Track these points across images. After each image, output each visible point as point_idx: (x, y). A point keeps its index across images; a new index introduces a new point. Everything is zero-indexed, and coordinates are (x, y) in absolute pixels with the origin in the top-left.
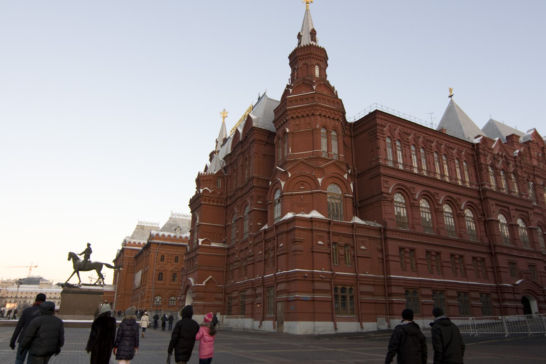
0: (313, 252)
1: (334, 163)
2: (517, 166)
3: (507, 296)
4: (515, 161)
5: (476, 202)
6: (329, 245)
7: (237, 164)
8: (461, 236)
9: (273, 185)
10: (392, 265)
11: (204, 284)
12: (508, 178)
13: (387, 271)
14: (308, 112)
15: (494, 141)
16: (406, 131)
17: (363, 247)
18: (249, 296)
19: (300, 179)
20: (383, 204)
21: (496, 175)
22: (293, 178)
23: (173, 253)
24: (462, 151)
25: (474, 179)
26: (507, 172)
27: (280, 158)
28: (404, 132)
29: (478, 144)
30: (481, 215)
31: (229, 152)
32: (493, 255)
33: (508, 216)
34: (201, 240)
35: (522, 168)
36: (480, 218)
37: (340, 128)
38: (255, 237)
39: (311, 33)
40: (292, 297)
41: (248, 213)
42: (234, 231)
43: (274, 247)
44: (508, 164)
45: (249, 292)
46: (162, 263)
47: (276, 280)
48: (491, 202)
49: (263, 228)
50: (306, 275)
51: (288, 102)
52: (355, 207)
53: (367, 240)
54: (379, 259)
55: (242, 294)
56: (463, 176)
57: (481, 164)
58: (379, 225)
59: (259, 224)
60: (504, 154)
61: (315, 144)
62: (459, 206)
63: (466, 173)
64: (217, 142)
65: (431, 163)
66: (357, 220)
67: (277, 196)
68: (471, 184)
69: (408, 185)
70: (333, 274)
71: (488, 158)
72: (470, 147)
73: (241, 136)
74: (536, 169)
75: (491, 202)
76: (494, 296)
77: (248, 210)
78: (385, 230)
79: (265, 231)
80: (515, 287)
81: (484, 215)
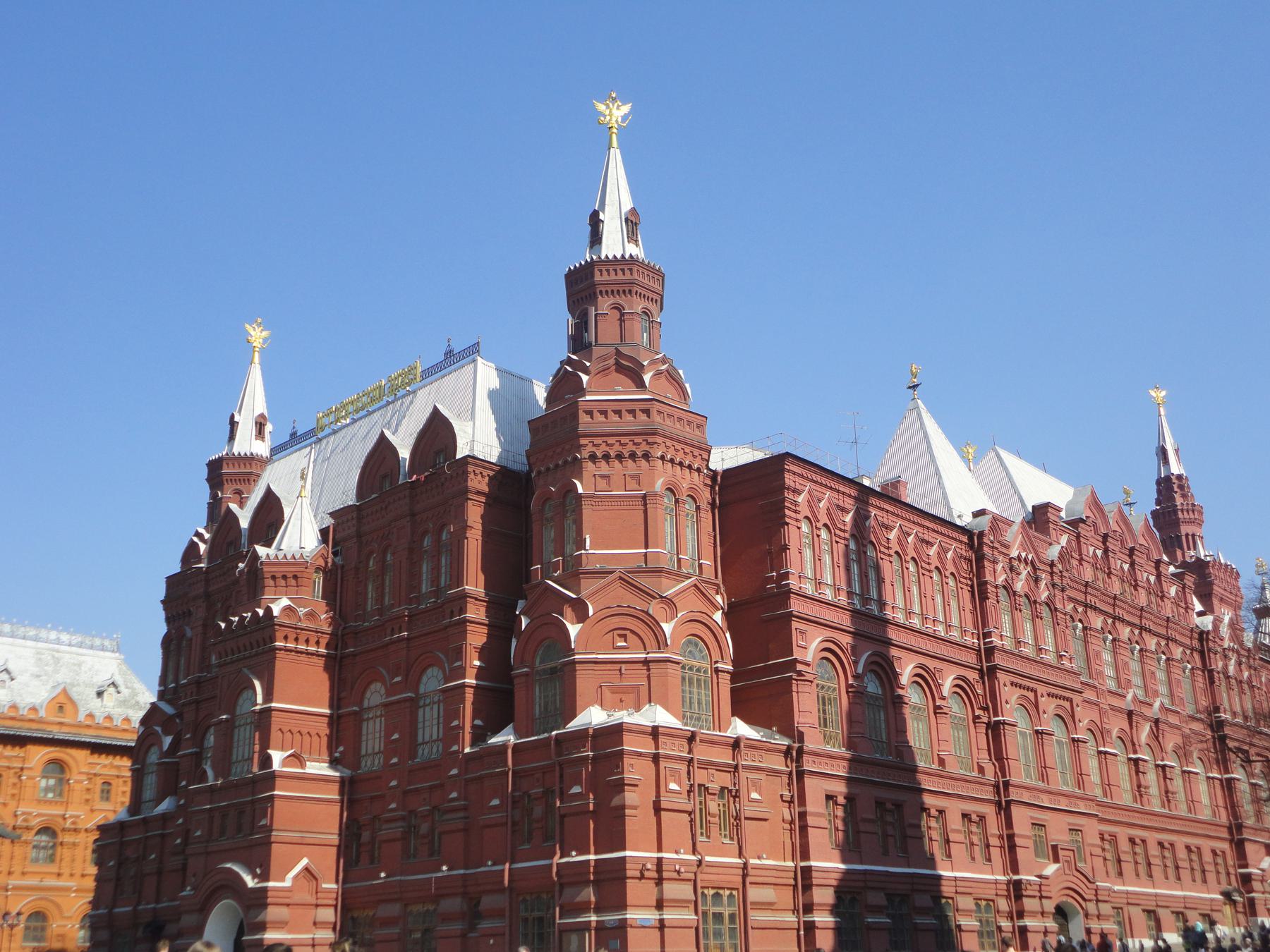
1: (695, 586)
2: (1054, 585)
4: (1052, 574)
15: (1009, 523)
16: (841, 504)
17: (754, 795)
20: (794, 688)
24: (948, 550)
26: (1035, 602)
28: (838, 506)
35: (1063, 590)
45: (453, 904)
53: (762, 776)
57: (986, 582)
60: (1030, 557)
71: (999, 567)
72: (965, 539)
74: (1089, 590)
80: (1044, 881)
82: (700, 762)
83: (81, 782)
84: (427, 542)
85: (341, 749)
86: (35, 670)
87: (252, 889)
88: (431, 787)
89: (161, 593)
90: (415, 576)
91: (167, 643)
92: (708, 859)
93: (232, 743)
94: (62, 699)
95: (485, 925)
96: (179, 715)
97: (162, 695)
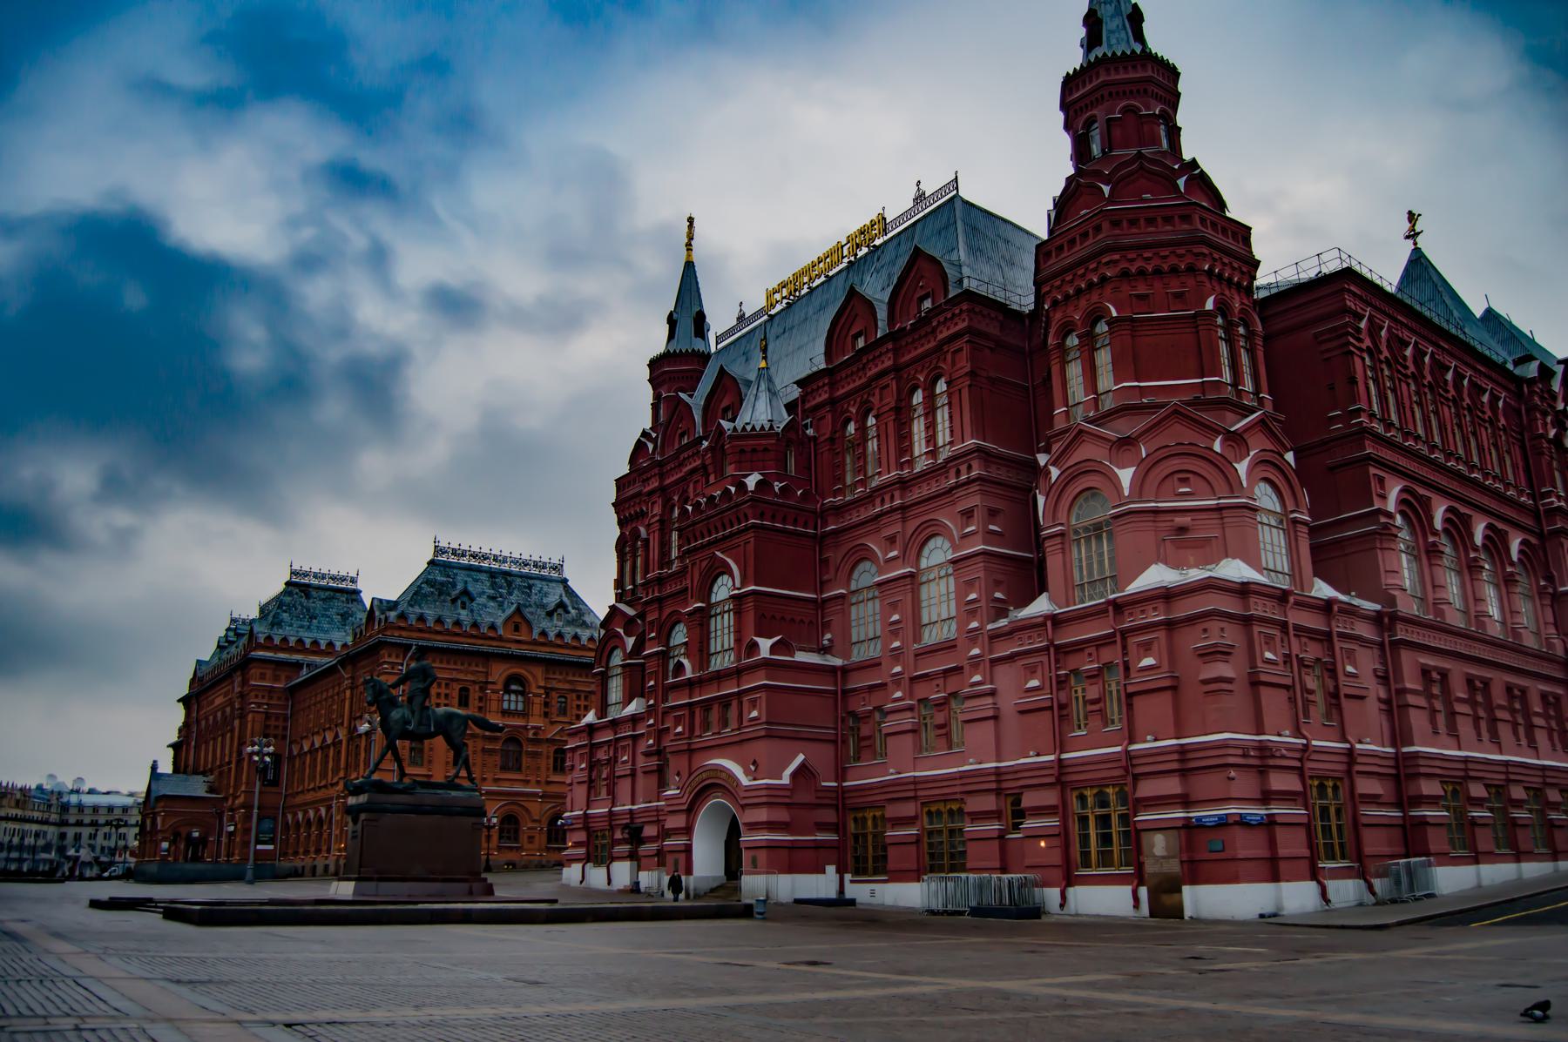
5: (1533, 540)
8: (1515, 633)
9: (1069, 478)
10: (1418, 720)
13: (1399, 735)
18: (977, 816)
19: (1176, 464)
23: (455, 675)
34: (765, 645)
36: (1545, 587)
39: (1129, 17)
41: (954, 562)
52: (1315, 549)
54: (1380, 700)
58: (1370, 606)
59: (998, 595)
61: (1207, 365)
64: (672, 321)
70: (1306, 747)
77: (937, 553)
78: (1395, 618)
81: (1550, 578)
82: (1297, 628)
83: (539, 695)
84: (918, 397)
85: (828, 636)
87: (748, 789)
88: (945, 671)
90: (905, 438)
91: (621, 546)
92: (1314, 743)
93: (709, 633)
95: (1030, 823)
96: (642, 615)
97: (619, 598)
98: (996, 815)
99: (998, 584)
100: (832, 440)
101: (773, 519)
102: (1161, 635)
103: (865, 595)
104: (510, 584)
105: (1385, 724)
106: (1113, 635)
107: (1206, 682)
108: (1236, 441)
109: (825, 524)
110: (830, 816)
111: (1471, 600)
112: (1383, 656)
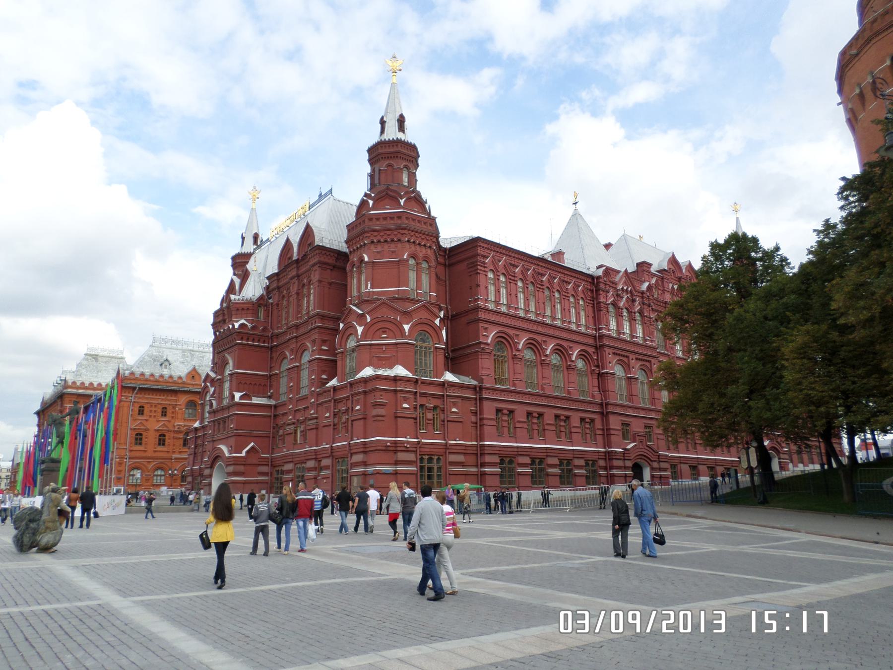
0: (396, 417)
3: (616, 463)
4: (643, 297)
5: (591, 350)
6: (415, 408)
7: (288, 289)
8: (569, 392)
9: (346, 328)
10: (487, 429)
11: (243, 454)
12: (632, 320)
14: (392, 236)
15: (618, 272)
17: (454, 410)
18: (310, 470)
19: (381, 325)
21: (619, 316)
22: (372, 324)
25: (591, 320)
27: (355, 294)
28: (511, 264)
29: (598, 278)
30: (595, 366)
31: (276, 271)
32: (604, 415)
33: (627, 367)
34: (237, 395)
37: (432, 257)
38: (319, 394)
39: (398, 120)
40: (370, 469)
41: (309, 362)
42: (284, 384)
43: (347, 410)
44: (633, 301)
45: (311, 464)
46: (140, 417)
47: (351, 450)
48: (607, 350)
49: (330, 384)
50: (389, 444)
51: (367, 220)
55: (298, 466)
56: (578, 319)
58: (474, 383)
59: (324, 376)
61: (401, 280)
62: (570, 355)
63: (582, 313)
64: (243, 238)
65: (541, 302)
66: (449, 377)
67: (352, 343)
68: (587, 328)
69: (511, 332)
73: (295, 249)
75: (607, 350)
76: (602, 463)
77: (306, 357)
78: (481, 388)
79: (335, 389)
82: (420, 393)
86: (182, 360)
89: (211, 320)
94: (194, 373)
95: (323, 473)
98: (315, 469)
99: (324, 372)
100: (278, 305)
101: (248, 340)
102: (362, 397)
103: (285, 374)
104: (192, 355)
105: (474, 432)
106: (348, 397)
107: (374, 416)
108: (407, 315)
109: (272, 342)
110: (265, 469)
111: (540, 377)
112: (476, 404)
